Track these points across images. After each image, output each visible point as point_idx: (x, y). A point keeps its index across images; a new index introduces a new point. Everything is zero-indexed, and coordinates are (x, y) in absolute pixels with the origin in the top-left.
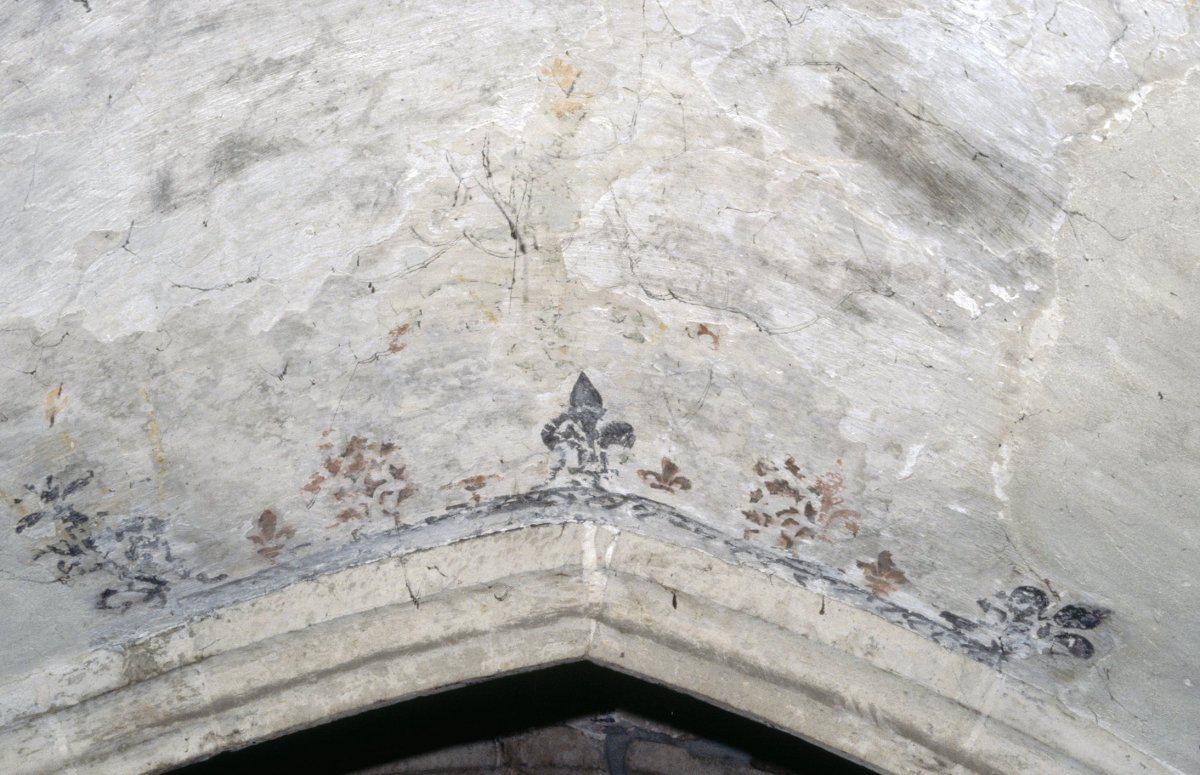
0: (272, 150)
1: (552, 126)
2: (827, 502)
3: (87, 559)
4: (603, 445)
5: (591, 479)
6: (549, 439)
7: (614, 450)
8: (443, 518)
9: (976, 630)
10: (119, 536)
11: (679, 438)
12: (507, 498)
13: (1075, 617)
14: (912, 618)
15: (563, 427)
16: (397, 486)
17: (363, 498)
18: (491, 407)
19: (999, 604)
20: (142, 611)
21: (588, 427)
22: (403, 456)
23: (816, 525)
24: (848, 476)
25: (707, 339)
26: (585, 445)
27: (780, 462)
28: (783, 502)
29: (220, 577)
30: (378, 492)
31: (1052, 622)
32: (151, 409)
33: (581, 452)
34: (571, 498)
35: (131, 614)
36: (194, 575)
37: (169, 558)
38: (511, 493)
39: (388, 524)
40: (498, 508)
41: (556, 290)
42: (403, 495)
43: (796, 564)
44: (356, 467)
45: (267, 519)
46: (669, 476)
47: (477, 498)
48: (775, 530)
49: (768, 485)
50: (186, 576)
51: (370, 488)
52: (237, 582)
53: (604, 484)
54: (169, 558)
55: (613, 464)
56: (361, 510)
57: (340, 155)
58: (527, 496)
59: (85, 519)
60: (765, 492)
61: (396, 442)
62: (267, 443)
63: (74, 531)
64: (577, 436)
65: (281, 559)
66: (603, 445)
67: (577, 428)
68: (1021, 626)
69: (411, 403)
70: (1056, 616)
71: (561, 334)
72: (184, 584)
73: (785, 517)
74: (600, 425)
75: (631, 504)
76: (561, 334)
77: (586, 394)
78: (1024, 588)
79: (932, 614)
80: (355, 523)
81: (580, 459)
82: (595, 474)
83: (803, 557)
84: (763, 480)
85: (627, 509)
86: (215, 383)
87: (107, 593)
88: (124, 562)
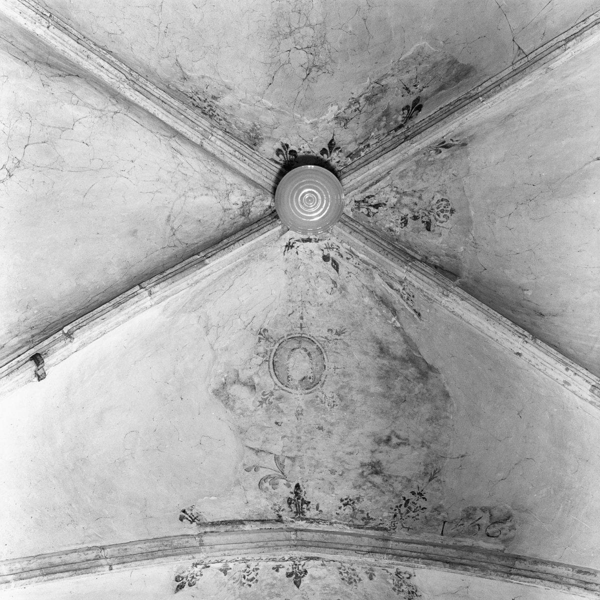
2: (241, 582)
3: (411, 589)
4: (293, 572)
6: (306, 572)
7: (291, 571)
10: (403, 591)
11: (275, 578)
13: (182, 586)
18: (319, 581)
19: (198, 578)
21: (297, 575)
22: (340, 576)
23: (242, 574)
26: (297, 571)
27: (253, 585)
28: (250, 577)
33: (298, 569)
34: (300, 559)
36: (389, 574)
37: (394, 580)
42: (340, 568)
45: (371, 578)
46: (277, 569)
48: (251, 568)
49: (254, 578)
50: (391, 574)
51: (347, 573)
52: (380, 566)
53: (293, 563)
54: (394, 580)
58: (311, 559)
60: (255, 577)
64: (299, 573)
65: (370, 567)
66: (293, 572)
68: (192, 576)
69: (337, 586)
70: (185, 583)
73: (250, 573)
74: (294, 576)
75: (286, 559)
77: (297, 584)
79: (212, 565)
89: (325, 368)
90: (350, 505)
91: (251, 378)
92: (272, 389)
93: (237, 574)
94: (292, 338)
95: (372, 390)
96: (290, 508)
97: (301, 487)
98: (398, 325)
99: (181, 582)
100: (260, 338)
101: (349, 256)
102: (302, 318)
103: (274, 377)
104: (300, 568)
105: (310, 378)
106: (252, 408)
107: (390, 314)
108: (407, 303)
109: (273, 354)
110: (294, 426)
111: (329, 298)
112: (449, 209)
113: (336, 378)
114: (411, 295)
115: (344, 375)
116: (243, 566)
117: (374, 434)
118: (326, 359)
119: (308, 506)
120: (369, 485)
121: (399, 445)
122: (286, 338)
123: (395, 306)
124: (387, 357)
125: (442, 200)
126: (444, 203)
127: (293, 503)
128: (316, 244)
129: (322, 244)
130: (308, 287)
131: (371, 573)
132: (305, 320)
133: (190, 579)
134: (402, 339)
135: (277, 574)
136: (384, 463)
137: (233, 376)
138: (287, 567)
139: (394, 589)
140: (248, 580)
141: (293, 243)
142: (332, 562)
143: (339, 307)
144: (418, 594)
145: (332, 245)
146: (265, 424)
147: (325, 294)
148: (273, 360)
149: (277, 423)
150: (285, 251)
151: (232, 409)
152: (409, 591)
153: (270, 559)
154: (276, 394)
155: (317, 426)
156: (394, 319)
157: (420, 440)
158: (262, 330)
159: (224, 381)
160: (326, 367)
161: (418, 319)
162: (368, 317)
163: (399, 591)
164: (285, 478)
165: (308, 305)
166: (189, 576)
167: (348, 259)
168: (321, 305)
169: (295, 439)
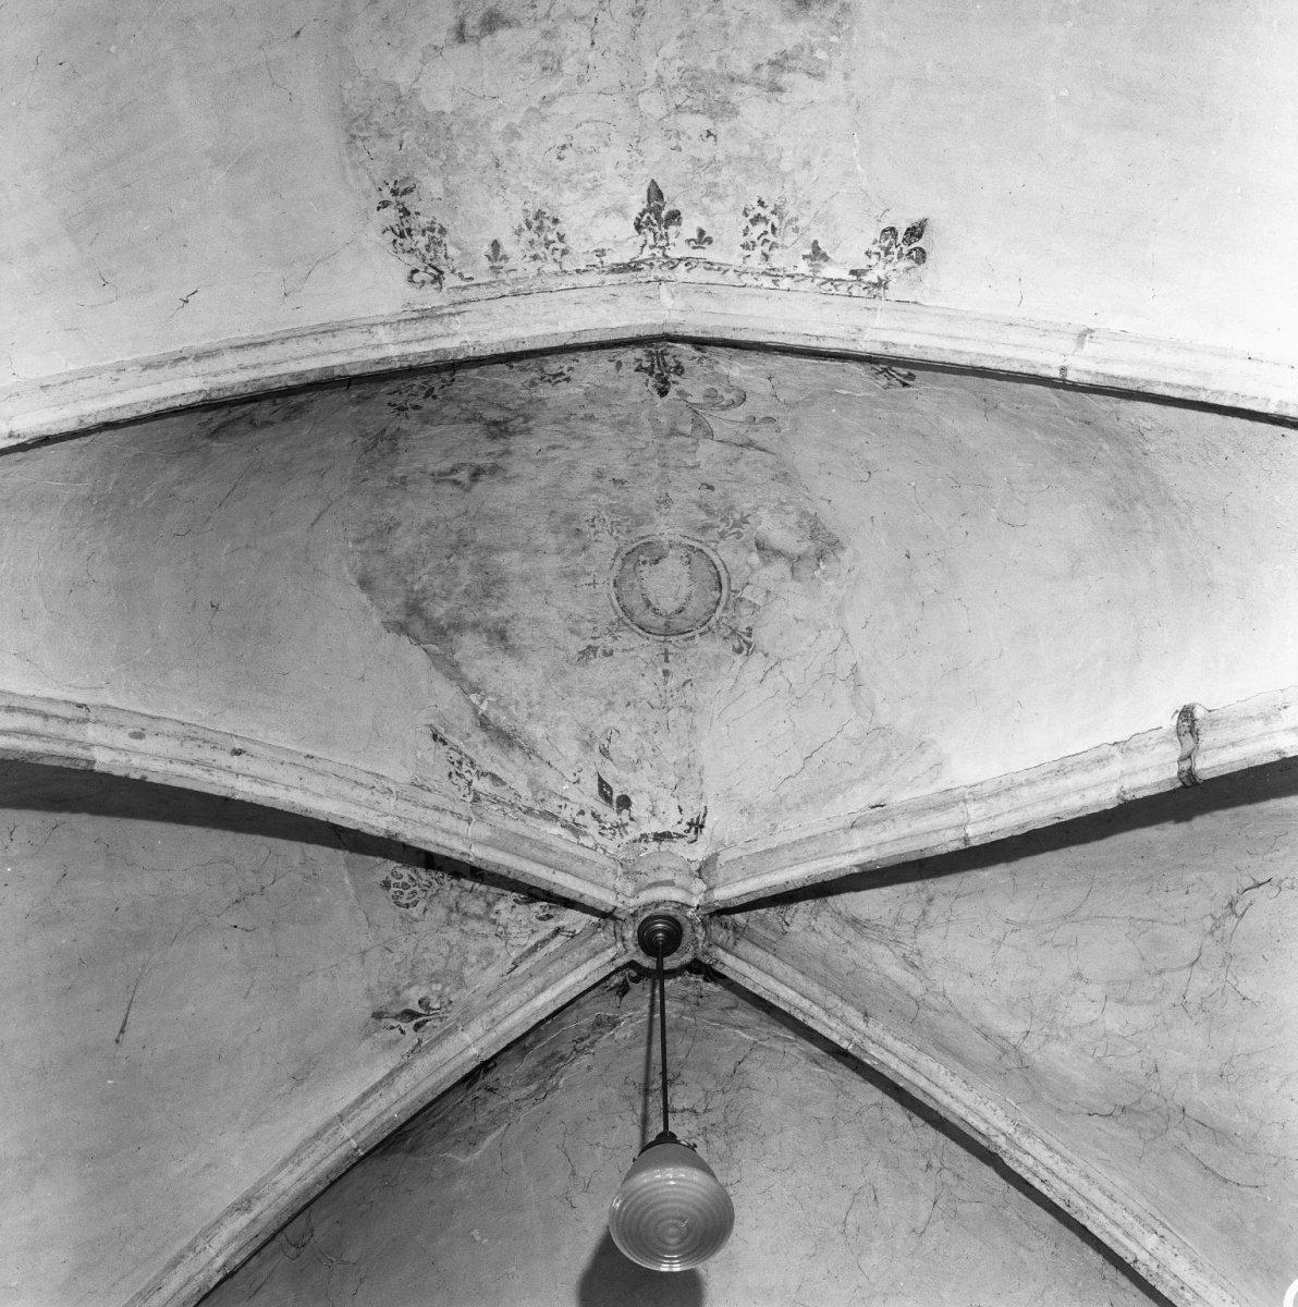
0: (507, 23)
1: (632, 21)
2: (781, 218)
3: (407, 242)
4: (666, 227)
5: (661, 251)
6: (638, 227)
7: (672, 229)
8: (585, 271)
9: (868, 273)
11: (705, 211)
12: (618, 265)
13: (912, 234)
14: (836, 283)
15: (645, 219)
16: (561, 246)
17: (544, 249)
19: (875, 249)
20: (430, 289)
22: (562, 228)
24: (788, 195)
25: (711, 138)
26: (656, 229)
27: (755, 204)
28: (761, 228)
29: (471, 279)
30: (551, 247)
31: (902, 246)
32: (445, 157)
34: (652, 264)
35: (423, 291)
37: (446, 257)
38: (619, 262)
39: (556, 268)
40: (613, 271)
41: (637, 124)
43: (772, 273)
44: (540, 228)
45: (495, 245)
46: (702, 239)
47: (602, 262)
48: (757, 252)
50: (453, 272)
53: (668, 253)
55: (672, 240)
56: (542, 255)
57: (535, 34)
59: (409, 214)
60: (750, 226)
61: (561, 219)
62: (497, 199)
63: (404, 220)
66: (666, 227)
67: (652, 218)
68: (889, 257)
70: (904, 239)
71: (640, 153)
72: (452, 276)
73: (762, 239)
74: (664, 214)
75: (682, 265)
76: (640, 153)
77: (655, 193)
78: (884, 231)
79: (845, 275)
80: (539, 263)
81: (655, 239)
82: (662, 247)
83: (775, 266)
84: (748, 218)
85: (682, 266)
86: (475, 153)
87: (415, 271)
88: (424, 252)
89: (615, 583)
90: (550, 375)
91: (766, 563)
92: (722, 543)
93: (789, 240)
94: (684, 633)
95: (516, 555)
96: (676, 362)
97: (655, 393)
98: (474, 698)
99: (913, 246)
100: (750, 635)
101: (580, 820)
102: (666, 673)
103: (717, 562)
104: (651, 241)
105: (644, 563)
106: (763, 513)
107: (491, 716)
108: (460, 753)
109: (722, 605)
110: (674, 484)
111: (612, 720)
112: (393, 889)
113: (592, 569)
114: (454, 776)
115: (574, 575)
116: (778, 260)
117: (507, 480)
118: (614, 597)
119: (640, 365)
120: (511, 405)
121: (453, 471)
122: (696, 632)
123: (483, 736)
124: (490, 625)
125: (408, 906)
126: (403, 901)
127: (671, 367)
128: (645, 830)
129: (633, 832)
130: (657, 739)
131: (496, 260)
132: (660, 670)
133: (893, 249)
134: (464, 670)
135: (702, 222)
136: (482, 438)
137: (803, 570)
138: (680, 242)
139: (443, 231)
140: (766, 220)
141: (689, 831)
142: (583, 267)
143: (592, 703)
144: (390, 236)
145: (614, 834)
146: (734, 486)
147: (622, 726)
148: (721, 591)
149: (711, 488)
150: (705, 815)
151: (804, 514)
152: (411, 236)
153: (719, 269)
154: (713, 534)
155: (626, 485)
156: (484, 707)
157: (411, 488)
158: (745, 652)
159: (821, 563)
160: (612, 585)
161: (437, 727)
162: (535, 697)
163: (433, 230)
164: (691, 406)
165: (654, 701)
166: (895, 256)
167: (582, 813)
168: (629, 704)
169: (672, 463)
